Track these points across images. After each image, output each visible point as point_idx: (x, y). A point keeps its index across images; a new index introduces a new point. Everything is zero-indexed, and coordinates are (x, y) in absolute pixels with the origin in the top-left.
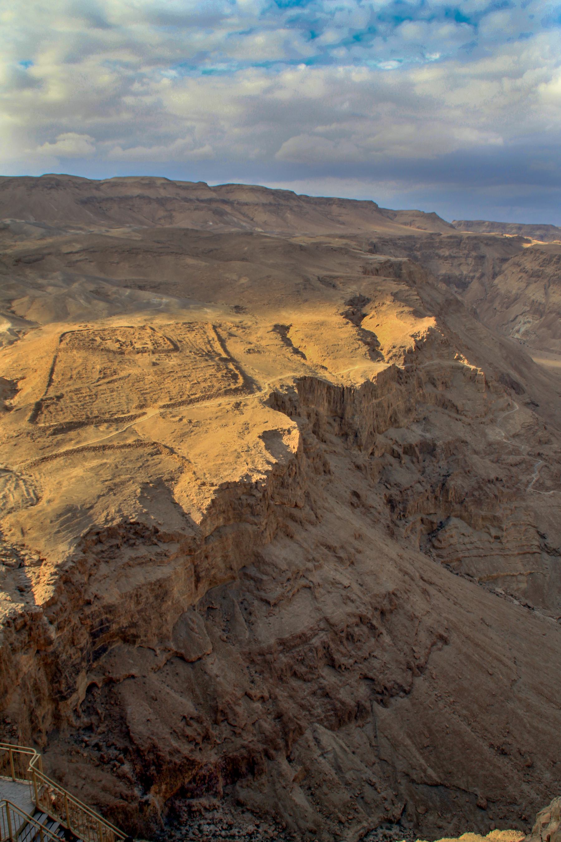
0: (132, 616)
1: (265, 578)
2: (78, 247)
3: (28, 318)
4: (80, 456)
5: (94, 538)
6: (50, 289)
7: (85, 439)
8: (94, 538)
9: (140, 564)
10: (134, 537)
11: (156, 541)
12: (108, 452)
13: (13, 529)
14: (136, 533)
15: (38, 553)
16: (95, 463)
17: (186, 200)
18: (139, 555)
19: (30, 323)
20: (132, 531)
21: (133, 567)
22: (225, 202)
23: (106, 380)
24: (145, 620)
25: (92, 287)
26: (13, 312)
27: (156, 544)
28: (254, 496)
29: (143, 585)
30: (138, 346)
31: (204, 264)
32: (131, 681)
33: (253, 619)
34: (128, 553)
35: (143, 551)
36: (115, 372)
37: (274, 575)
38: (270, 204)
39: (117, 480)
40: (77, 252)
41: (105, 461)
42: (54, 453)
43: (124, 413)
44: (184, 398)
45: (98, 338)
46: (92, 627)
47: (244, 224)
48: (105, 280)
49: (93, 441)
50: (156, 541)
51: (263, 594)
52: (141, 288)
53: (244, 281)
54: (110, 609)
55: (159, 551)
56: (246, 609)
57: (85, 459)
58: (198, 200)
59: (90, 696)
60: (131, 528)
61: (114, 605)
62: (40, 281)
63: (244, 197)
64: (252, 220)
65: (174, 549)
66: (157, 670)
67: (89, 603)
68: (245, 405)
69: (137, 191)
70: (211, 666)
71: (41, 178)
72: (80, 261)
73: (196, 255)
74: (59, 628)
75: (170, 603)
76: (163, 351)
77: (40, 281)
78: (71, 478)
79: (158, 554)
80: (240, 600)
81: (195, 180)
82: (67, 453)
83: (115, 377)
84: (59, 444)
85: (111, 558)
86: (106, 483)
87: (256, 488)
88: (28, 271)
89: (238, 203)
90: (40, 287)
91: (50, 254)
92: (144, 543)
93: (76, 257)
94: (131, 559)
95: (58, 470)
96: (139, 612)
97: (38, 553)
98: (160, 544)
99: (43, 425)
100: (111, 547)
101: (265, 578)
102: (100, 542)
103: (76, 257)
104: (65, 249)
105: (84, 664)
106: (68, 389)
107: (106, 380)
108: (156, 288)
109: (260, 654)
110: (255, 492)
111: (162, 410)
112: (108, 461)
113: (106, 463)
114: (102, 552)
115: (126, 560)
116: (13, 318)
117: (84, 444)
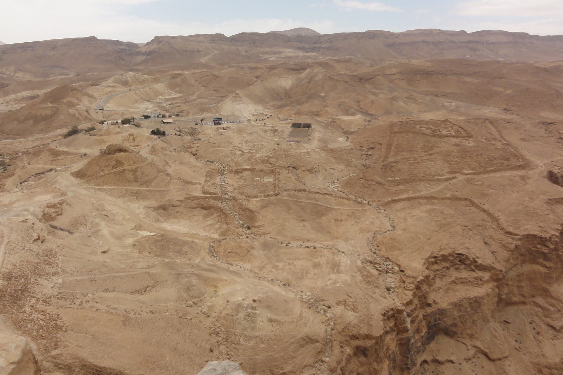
0: (455, 319)
1: (552, 308)
2: (395, 71)
3: (369, 112)
4: (417, 201)
5: (433, 260)
6: (381, 96)
7: (420, 191)
8: (433, 260)
9: (462, 283)
10: (459, 263)
11: (474, 268)
12: (436, 201)
13: (381, 246)
14: (460, 261)
15: (398, 265)
16: (428, 207)
17: (452, 42)
18: (462, 276)
19: (371, 115)
20: (458, 259)
21: (457, 284)
22: (477, 42)
23: (427, 153)
24: (462, 323)
25: (406, 95)
26: (361, 108)
27: (474, 271)
28: (548, 247)
29: (465, 299)
30: (444, 133)
31: (477, 81)
32: (450, 365)
33: (540, 338)
34: (454, 274)
35: (465, 274)
36: (431, 149)
37: (559, 307)
38: (510, 42)
39: (444, 222)
40: (394, 74)
41: (435, 207)
42: (400, 197)
43: (441, 176)
44: (482, 170)
45: (417, 126)
46: (430, 322)
47: (491, 56)
48: (413, 91)
49: (424, 193)
50: (474, 268)
51: (549, 321)
52: (437, 96)
53: (509, 92)
54: (442, 312)
55: (476, 276)
56: (534, 329)
57: (420, 204)
58: (460, 42)
59: (422, 369)
60: (457, 257)
61: (445, 310)
62: (375, 91)
63: (491, 39)
64: (496, 53)
65: (486, 276)
66: (468, 360)
67: (430, 305)
68: (528, 178)
69: (421, 39)
70: (508, 368)
71: (365, 32)
72: (396, 79)
73: (471, 75)
74: (412, 322)
75: (480, 314)
76: (462, 137)
77: (375, 91)
78: (413, 216)
79: (476, 278)
80: (529, 320)
81: (458, 29)
82: (408, 199)
83: (432, 152)
84: (402, 192)
85: (443, 275)
86: (438, 223)
87: (550, 241)
88: (367, 85)
89: (487, 43)
90: (375, 94)
91: (378, 75)
92: (465, 269)
93: (394, 77)
94: (457, 279)
95: (403, 209)
96: (460, 317)
97: (398, 265)
98: (476, 270)
99: (390, 179)
100: (444, 268)
101: (552, 308)
102: (436, 263)
103: (394, 77)
104: (388, 72)
105: (422, 347)
106: (402, 157)
107: (427, 153)
108: (444, 95)
109: (547, 367)
110: (549, 244)
111: (468, 176)
112: (437, 207)
113: (434, 209)
114: (438, 270)
115: (453, 279)
116: (361, 112)
117: (418, 194)
